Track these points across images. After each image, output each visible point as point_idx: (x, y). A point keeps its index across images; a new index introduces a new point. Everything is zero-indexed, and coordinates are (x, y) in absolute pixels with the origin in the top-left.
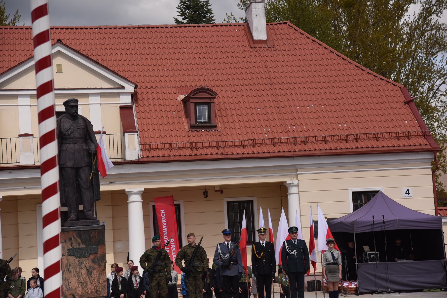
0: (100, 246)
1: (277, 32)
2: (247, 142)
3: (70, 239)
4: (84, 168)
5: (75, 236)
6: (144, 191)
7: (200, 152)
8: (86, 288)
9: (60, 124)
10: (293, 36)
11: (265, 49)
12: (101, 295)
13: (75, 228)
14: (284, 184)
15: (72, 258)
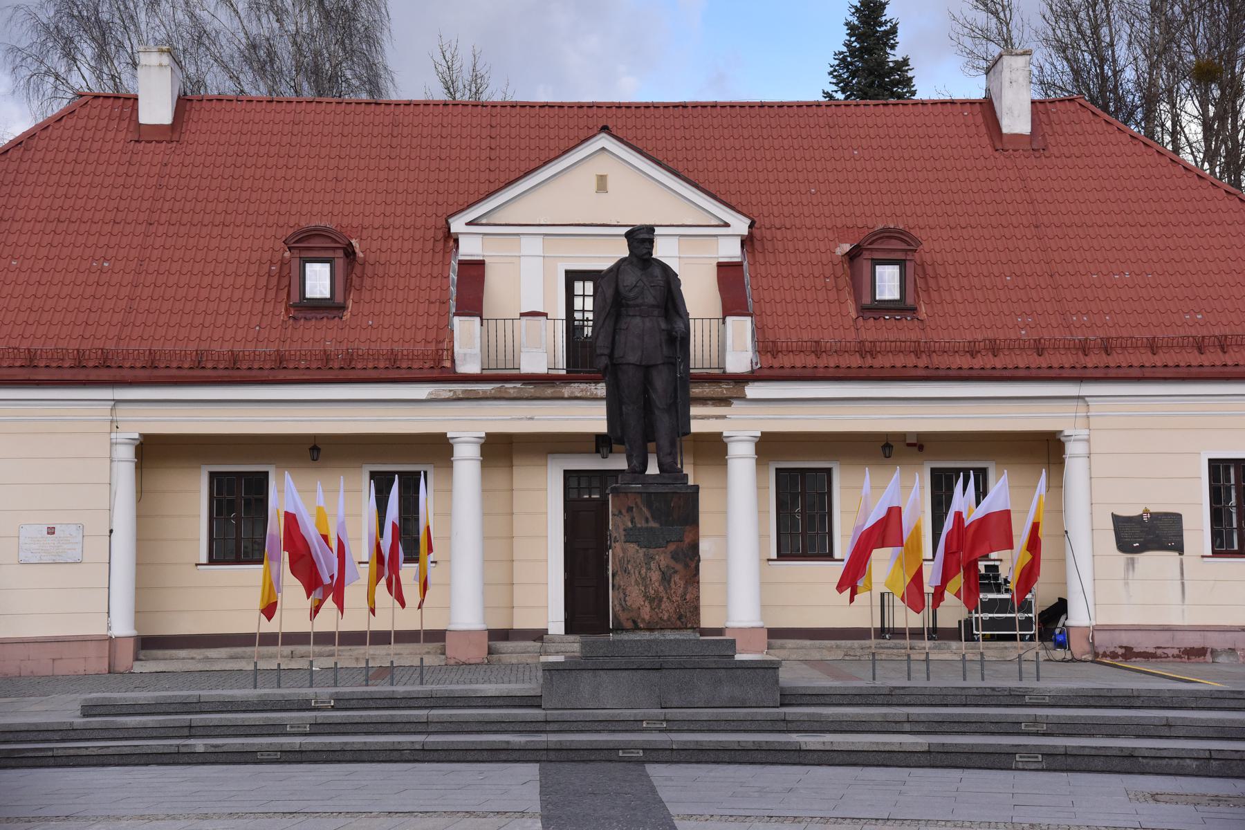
0: (688, 528)
2: (982, 344)
3: (630, 509)
5: (639, 503)
6: (760, 437)
7: (879, 361)
9: (617, 277)
10: (1088, 128)
11: (1026, 154)
12: (689, 626)
14: (1057, 437)
15: (632, 547)
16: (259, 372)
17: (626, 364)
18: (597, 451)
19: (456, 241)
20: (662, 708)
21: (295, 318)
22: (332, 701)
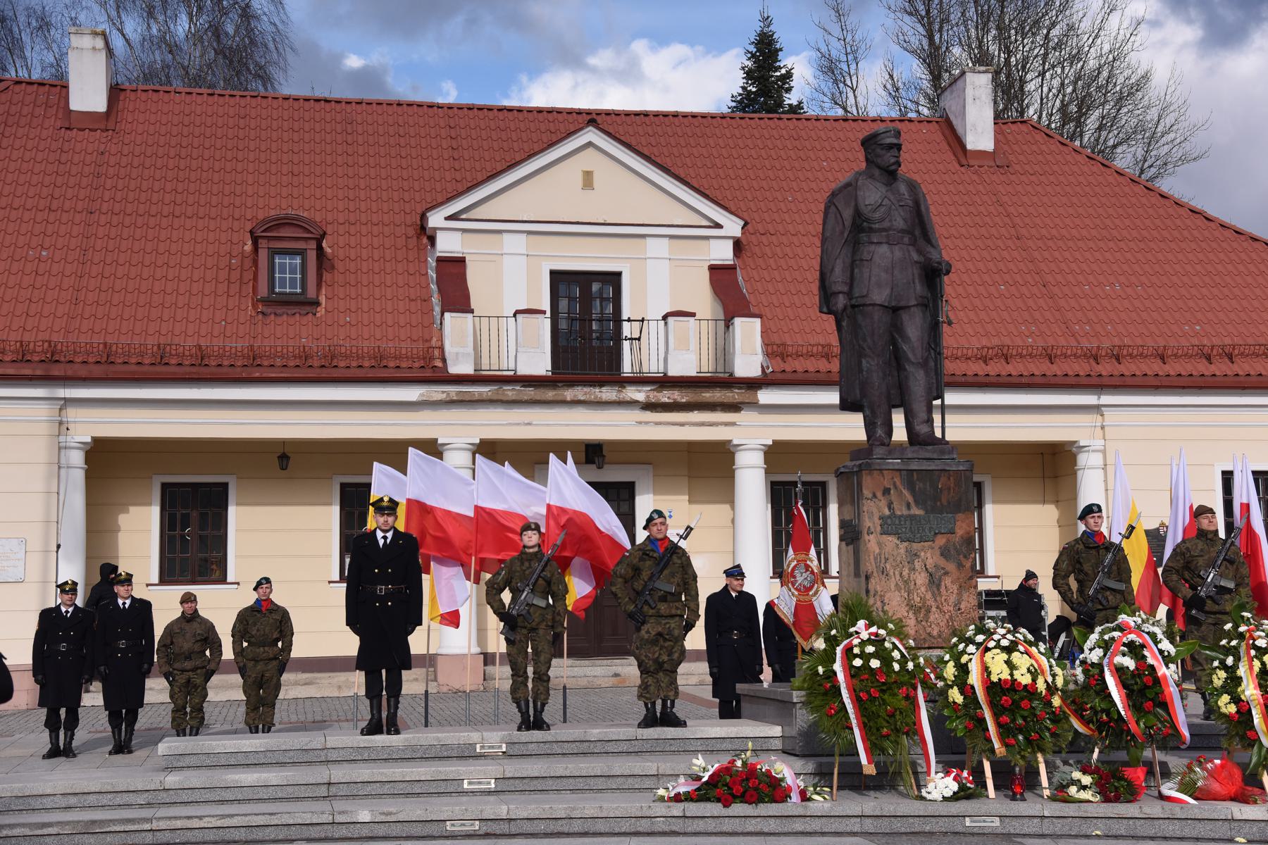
0: (960, 516)
1: (1010, 137)
3: (886, 491)
4: (912, 309)
5: (898, 483)
8: (927, 621)
10: (1044, 147)
13: (898, 463)
15: (891, 540)
16: (231, 369)
17: (870, 305)
19: (432, 240)
20: (953, 753)
21: (263, 313)
22: (504, 745)
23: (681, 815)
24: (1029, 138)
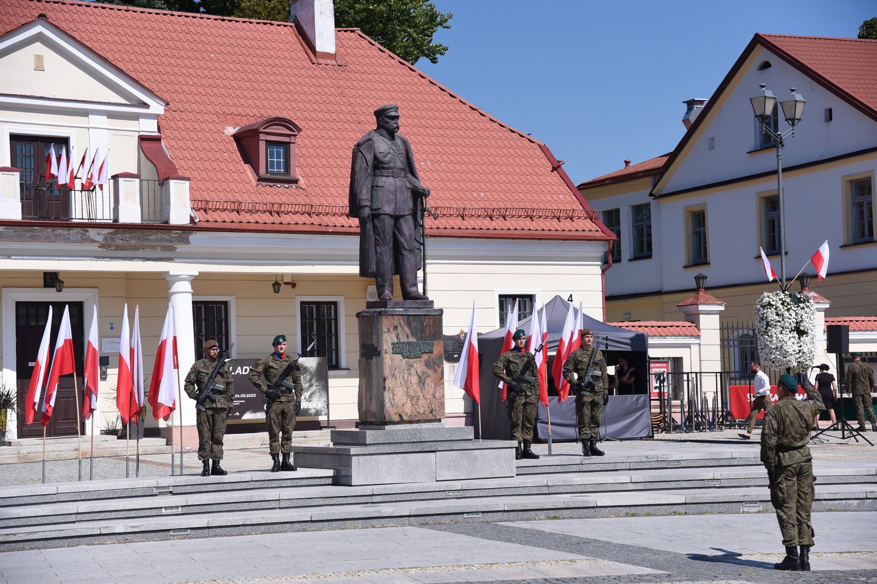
0: (435, 342)
3: (395, 328)
4: (407, 217)
5: (402, 323)
7: (286, 219)
13: (402, 311)
15: (399, 357)
18: (46, 285)
23: (310, 519)
24: (357, 43)
